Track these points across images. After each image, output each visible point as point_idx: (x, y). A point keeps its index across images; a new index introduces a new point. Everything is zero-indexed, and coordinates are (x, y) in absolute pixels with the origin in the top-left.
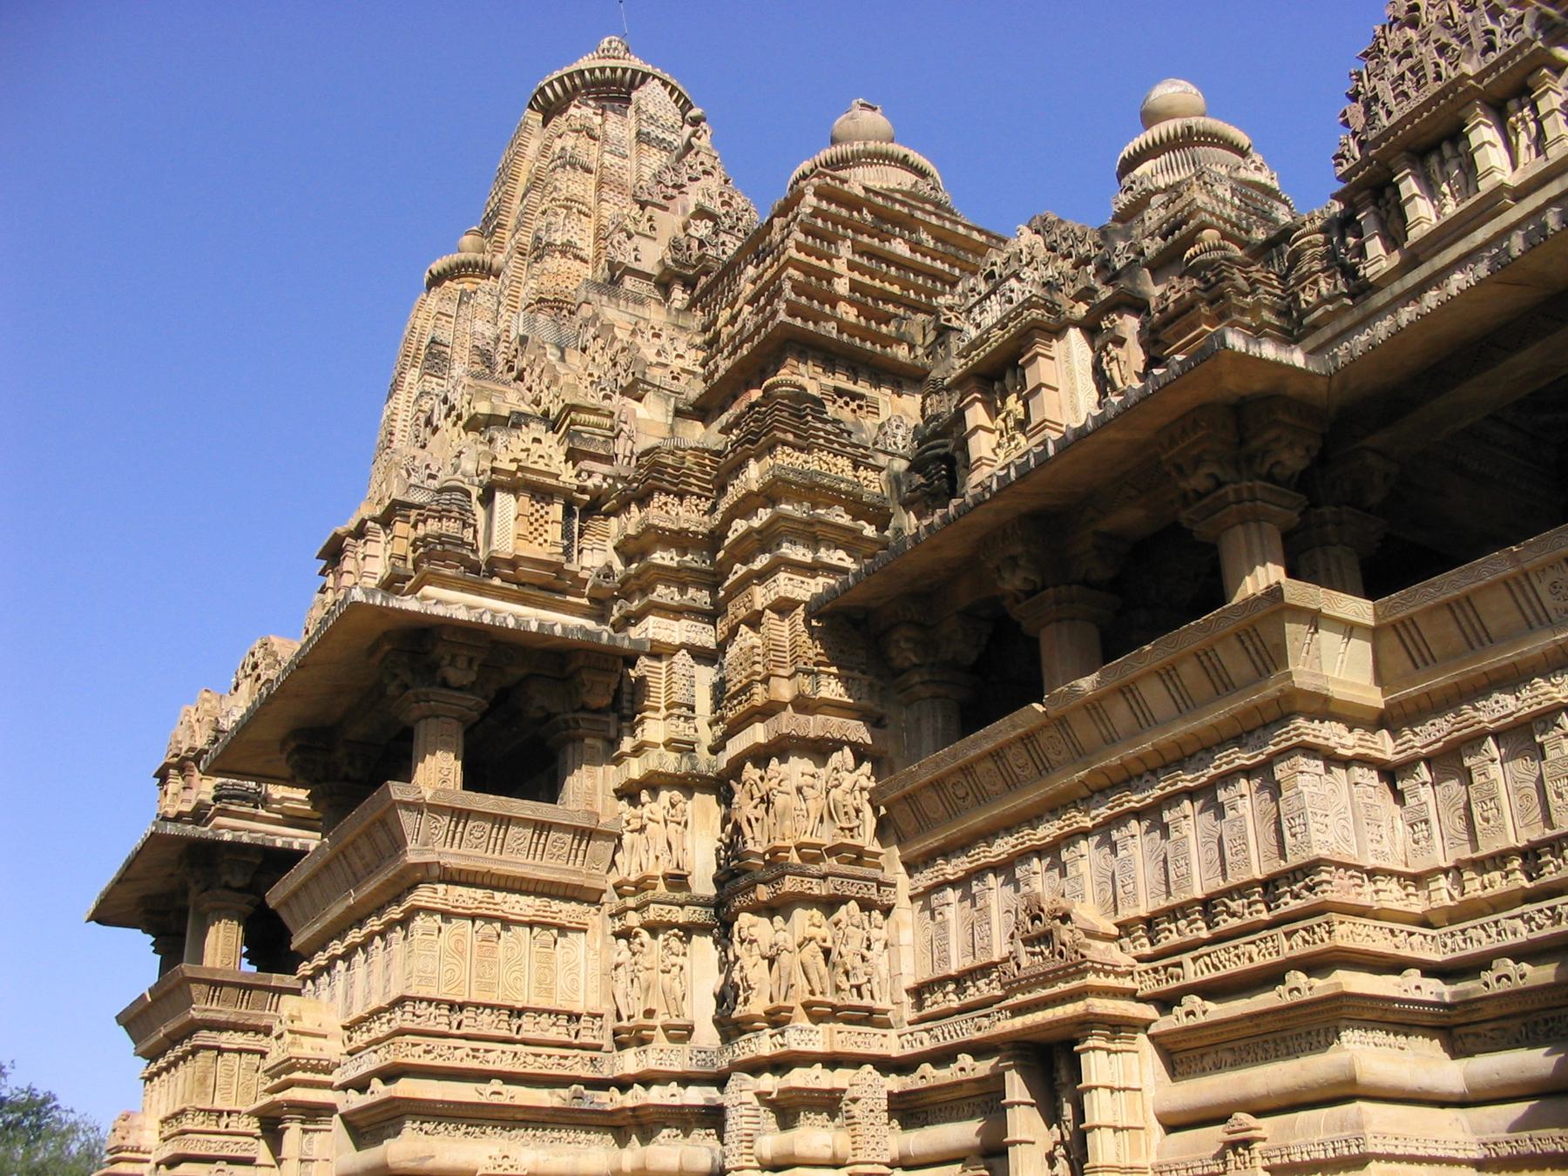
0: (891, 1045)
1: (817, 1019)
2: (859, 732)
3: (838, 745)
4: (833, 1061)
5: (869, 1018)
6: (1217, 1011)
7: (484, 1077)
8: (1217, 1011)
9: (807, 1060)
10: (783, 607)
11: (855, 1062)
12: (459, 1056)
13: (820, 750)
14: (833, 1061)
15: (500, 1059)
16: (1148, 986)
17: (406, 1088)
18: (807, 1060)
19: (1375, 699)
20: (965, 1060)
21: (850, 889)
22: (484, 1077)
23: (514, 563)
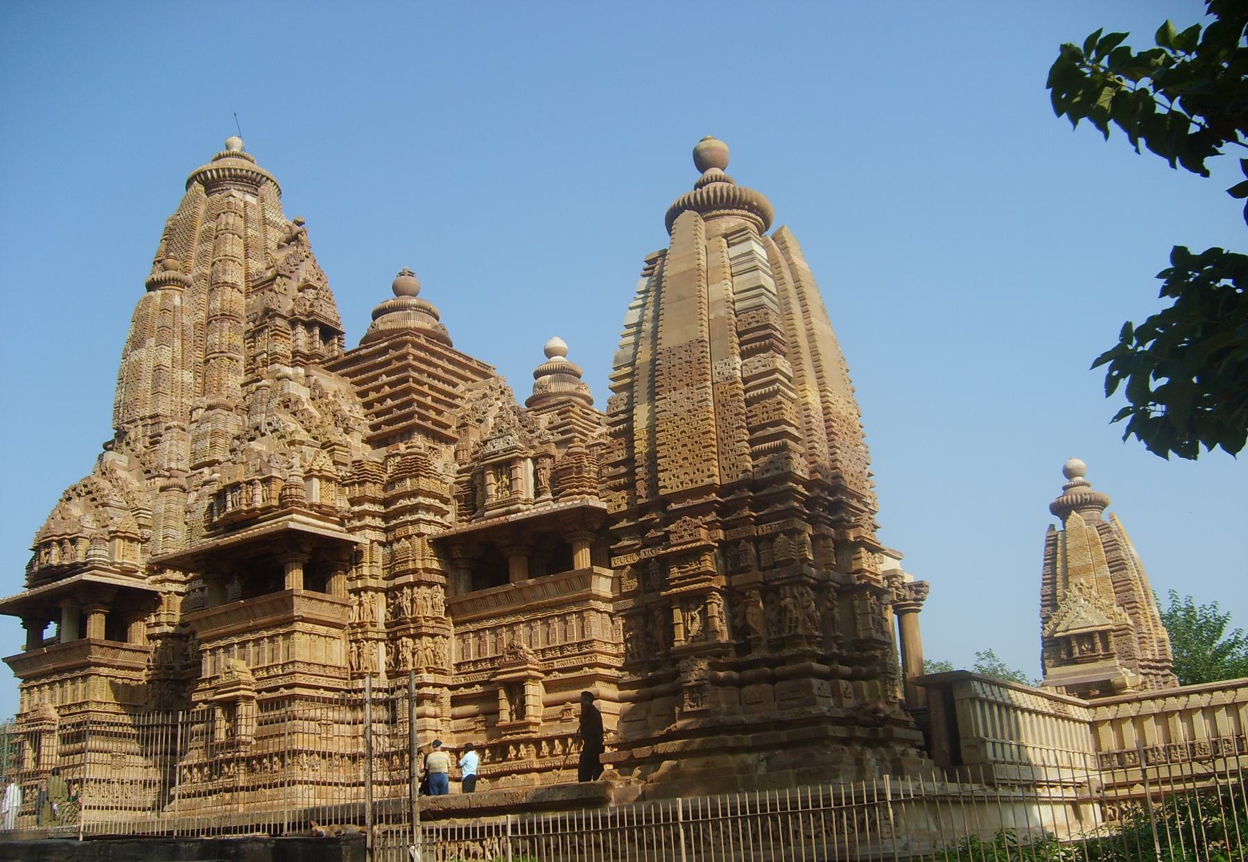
0: (448, 681)
1: (429, 672)
2: (442, 579)
3: (436, 584)
4: (435, 685)
5: (443, 672)
6: (562, 676)
7: (318, 688)
8: (562, 676)
9: (428, 685)
10: (420, 535)
11: (441, 686)
12: (311, 681)
13: (430, 585)
14: (435, 685)
15: (323, 682)
16: (543, 668)
17: (297, 691)
18: (428, 685)
19: (610, 596)
20: (478, 686)
21: (440, 632)
22: (318, 688)
23: (319, 507)
